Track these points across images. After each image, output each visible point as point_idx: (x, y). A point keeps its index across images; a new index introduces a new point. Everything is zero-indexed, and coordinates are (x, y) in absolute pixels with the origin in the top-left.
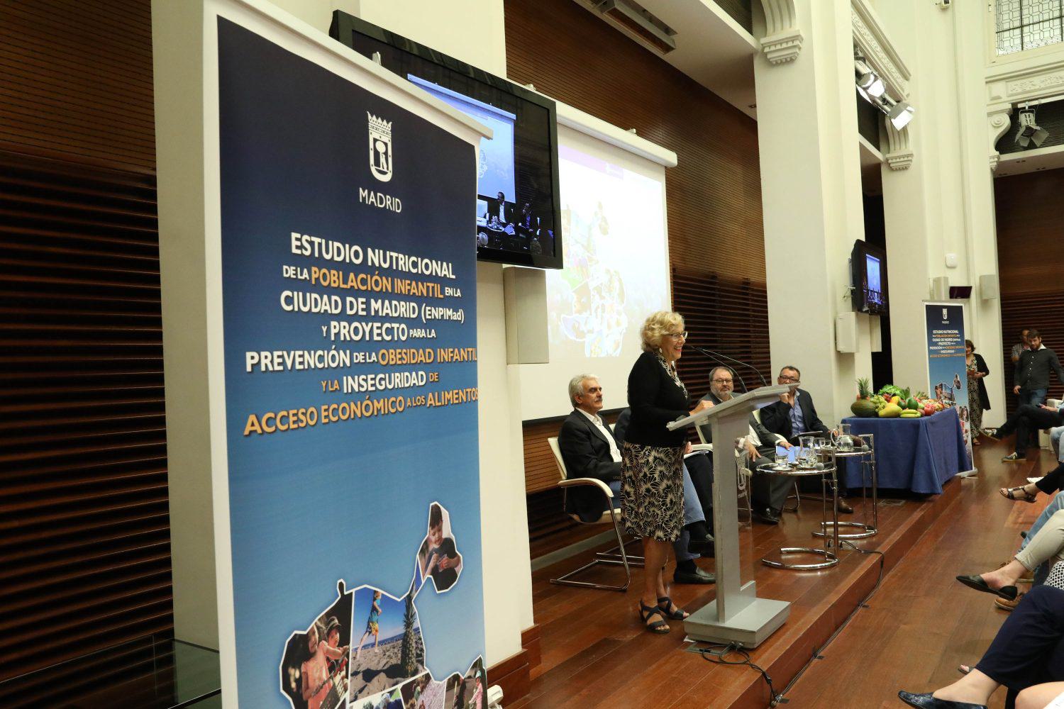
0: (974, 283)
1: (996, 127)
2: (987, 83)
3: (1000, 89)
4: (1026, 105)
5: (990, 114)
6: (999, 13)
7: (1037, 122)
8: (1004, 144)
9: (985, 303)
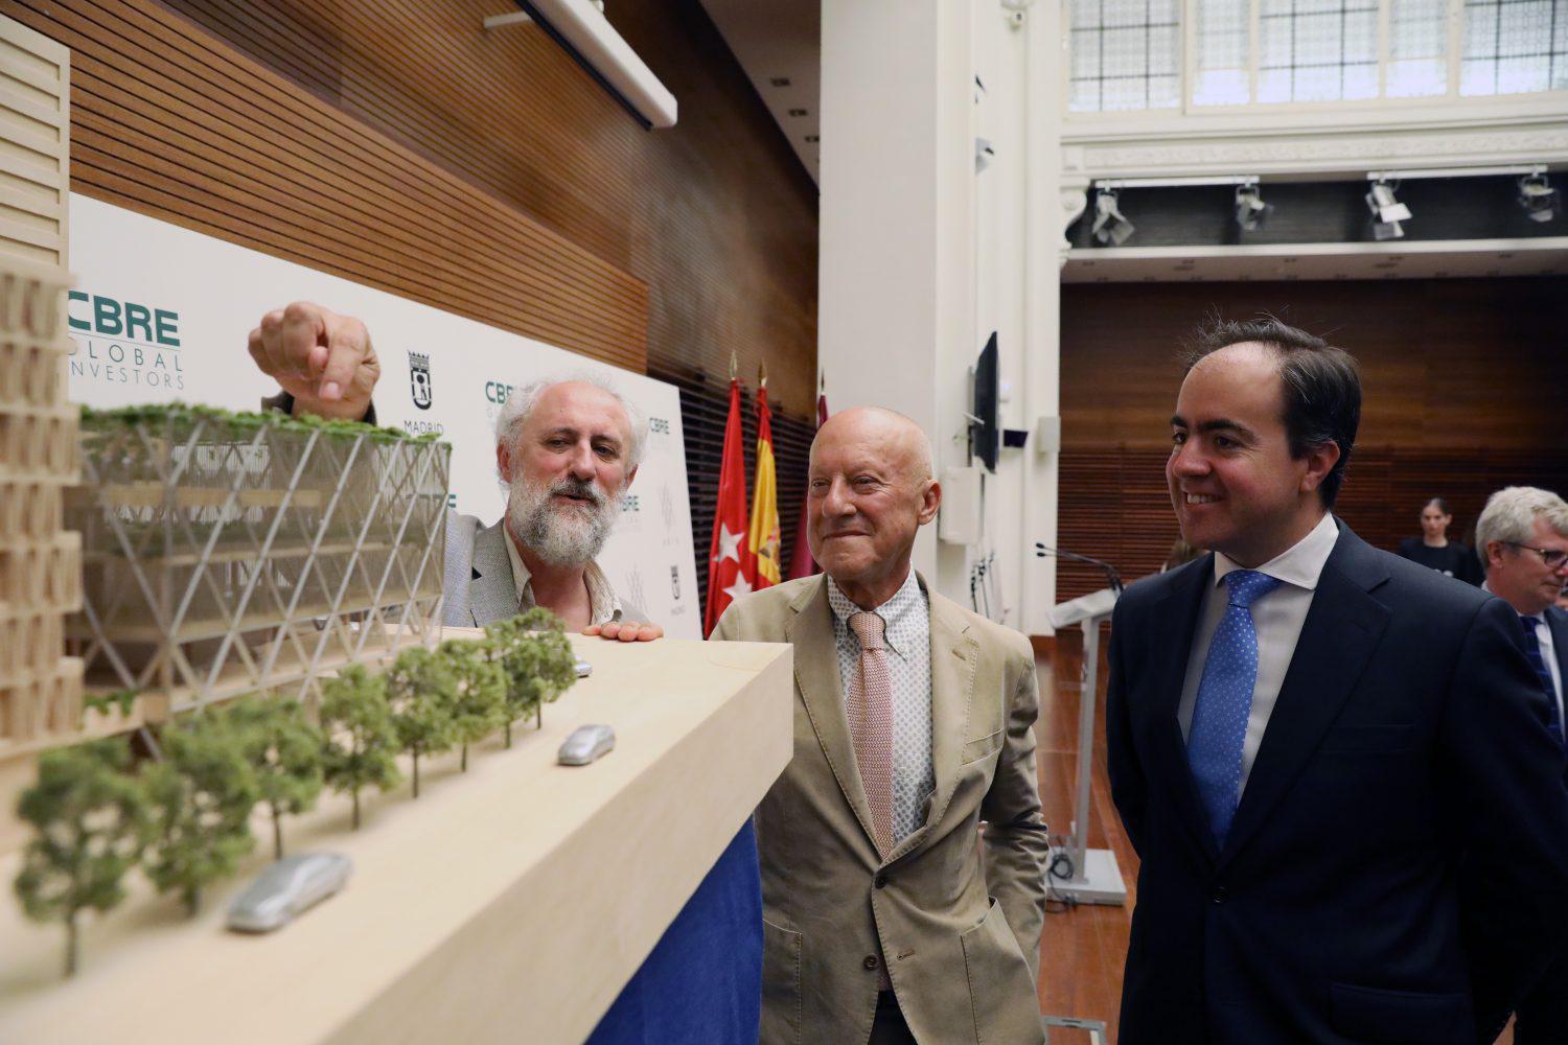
0: (1031, 427)
1: (1069, 208)
2: (1063, 144)
3: (1076, 155)
4: (1107, 185)
5: (1064, 189)
6: (1075, 54)
7: (1120, 208)
8: (1076, 233)
9: (1041, 456)
